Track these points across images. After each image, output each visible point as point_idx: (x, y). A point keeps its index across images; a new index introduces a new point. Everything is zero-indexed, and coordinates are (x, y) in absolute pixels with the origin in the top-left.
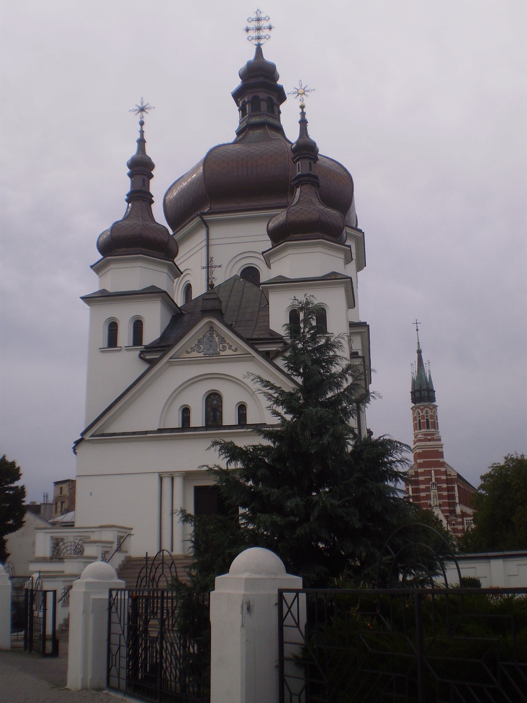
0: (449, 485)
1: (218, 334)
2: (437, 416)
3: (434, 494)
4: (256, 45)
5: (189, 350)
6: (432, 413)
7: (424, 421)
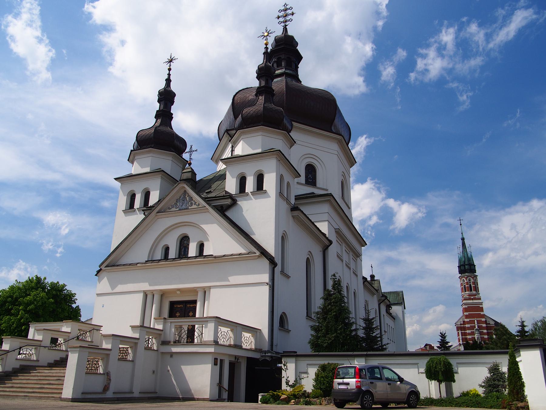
0: (489, 331)
1: (188, 195)
2: (477, 283)
3: (477, 337)
5: (170, 207)
6: (473, 280)
7: (468, 286)
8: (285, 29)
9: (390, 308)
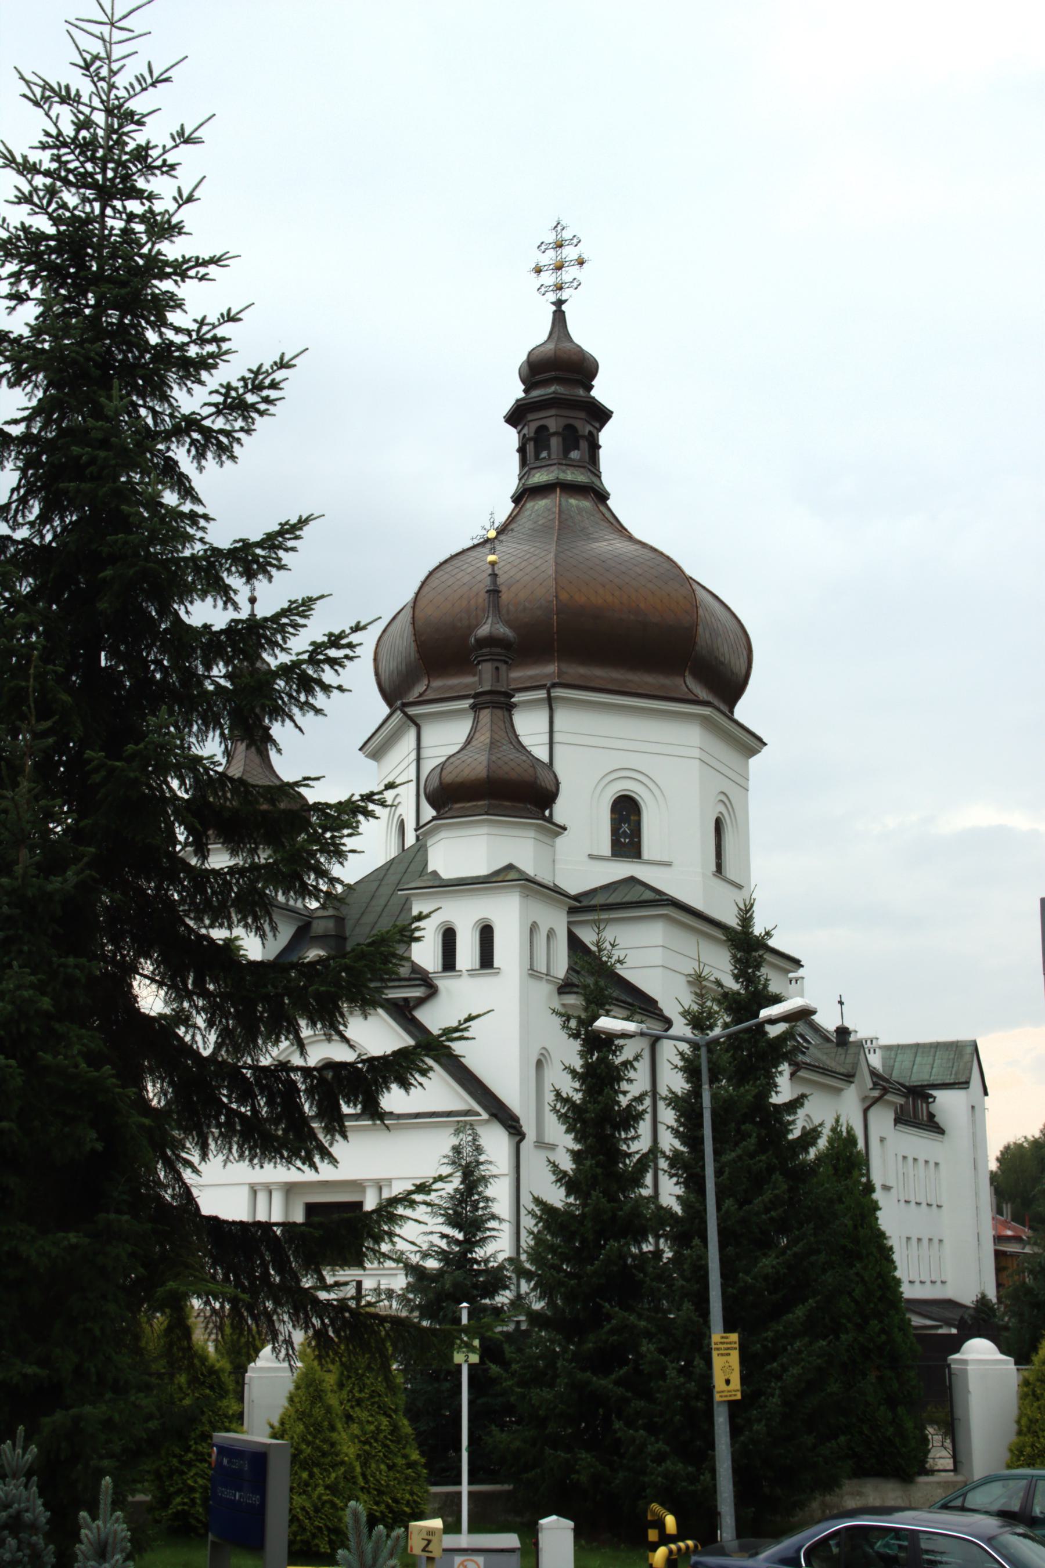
4: (553, 303)
8: (559, 317)
9: (931, 1100)
